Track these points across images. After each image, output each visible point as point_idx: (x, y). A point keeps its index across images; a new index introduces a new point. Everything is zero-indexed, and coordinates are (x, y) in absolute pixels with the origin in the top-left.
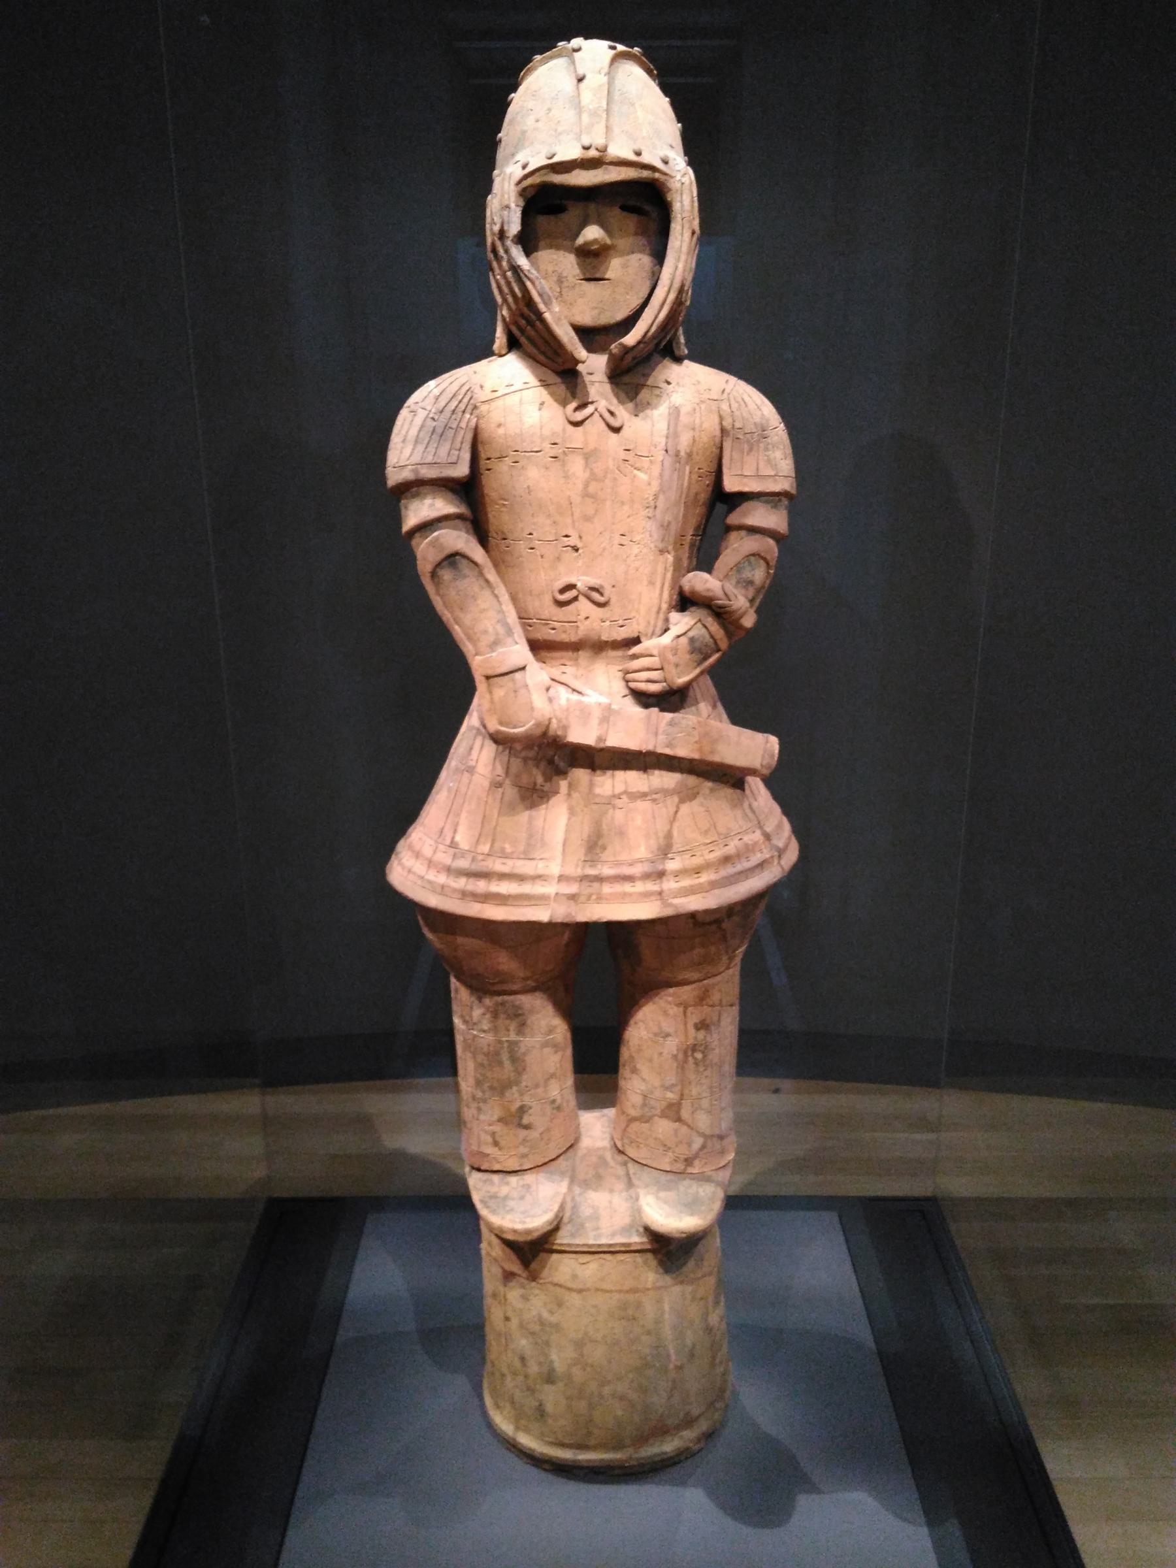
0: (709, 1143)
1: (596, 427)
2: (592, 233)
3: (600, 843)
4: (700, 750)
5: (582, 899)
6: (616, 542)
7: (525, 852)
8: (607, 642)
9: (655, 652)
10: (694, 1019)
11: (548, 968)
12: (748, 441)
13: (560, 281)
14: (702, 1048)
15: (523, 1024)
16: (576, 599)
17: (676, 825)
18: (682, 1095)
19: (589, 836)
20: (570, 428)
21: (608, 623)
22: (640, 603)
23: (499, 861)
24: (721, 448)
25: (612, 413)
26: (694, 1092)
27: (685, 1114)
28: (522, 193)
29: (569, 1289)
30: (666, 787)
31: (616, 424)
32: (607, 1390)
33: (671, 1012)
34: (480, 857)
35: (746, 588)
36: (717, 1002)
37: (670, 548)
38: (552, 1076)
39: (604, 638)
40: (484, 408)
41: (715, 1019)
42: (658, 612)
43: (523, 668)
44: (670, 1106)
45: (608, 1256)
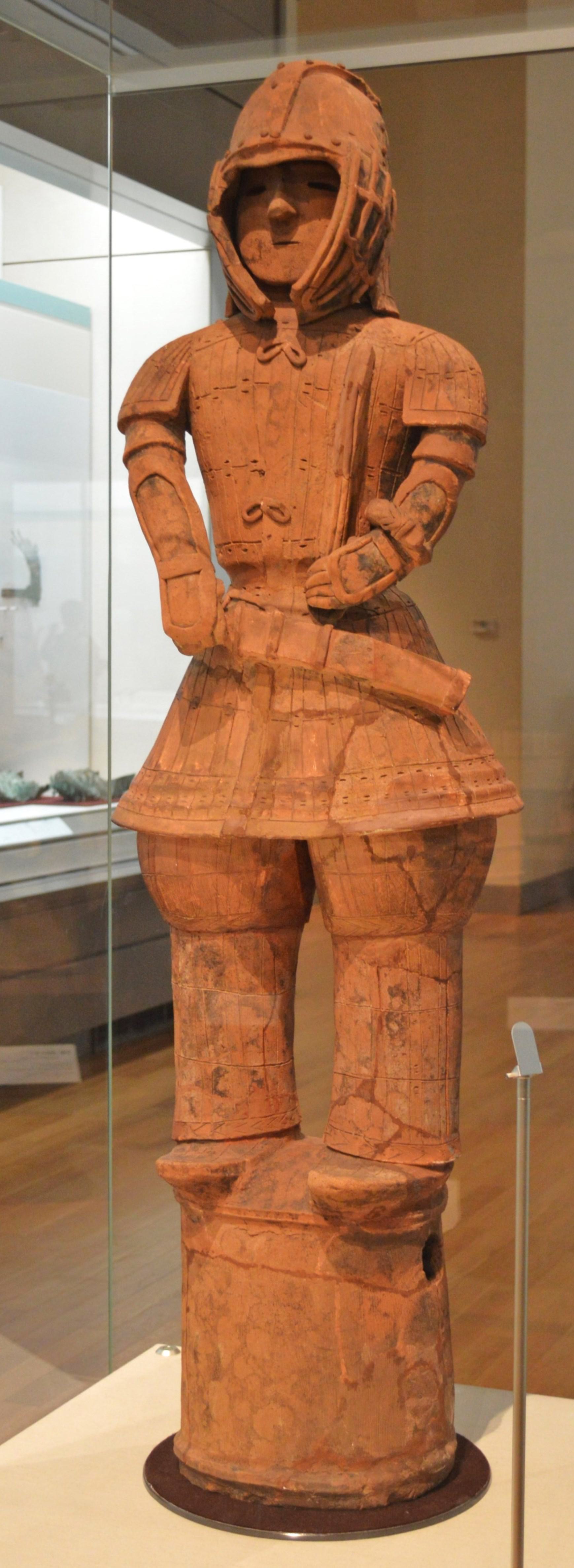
0: (405, 1133)
1: (281, 365)
2: (278, 203)
3: (276, 761)
4: (375, 670)
5: (254, 813)
6: (297, 466)
7: (210, 769)
8: (290, 561)
9: (325, 566)
10: (388, 982)
11: (243, 910)
12: (430, 381)
13: (260, 246)
14: (399, 1018)
15: (221, 974)
16: (260, 518)
17: (350, 746)
18: (376, 1071)
19: (267, 753)
20: (260, 366)
21: (290, 542)
22: (320, 525)
23: (188, 778)
24: (403, 387)
25: (297, 353)
26: (390, 1070)
27: (379, 1093)
28: (225, 177)
29: (239, 1265)
30: (342, 707)
31: (298, 360)
32: (269, 1392)
33: (365, 972)
34: (174, 776)
35: (420, 512)
36: (415, 967)
37: (345, 470)
38: (252, 1042)
39: (286, 556)
40: (195, 355)
41: (414, 986)
42: (334, 532)
43: (198, 573)
44: (365, 1082)
45: (276, 1229)
